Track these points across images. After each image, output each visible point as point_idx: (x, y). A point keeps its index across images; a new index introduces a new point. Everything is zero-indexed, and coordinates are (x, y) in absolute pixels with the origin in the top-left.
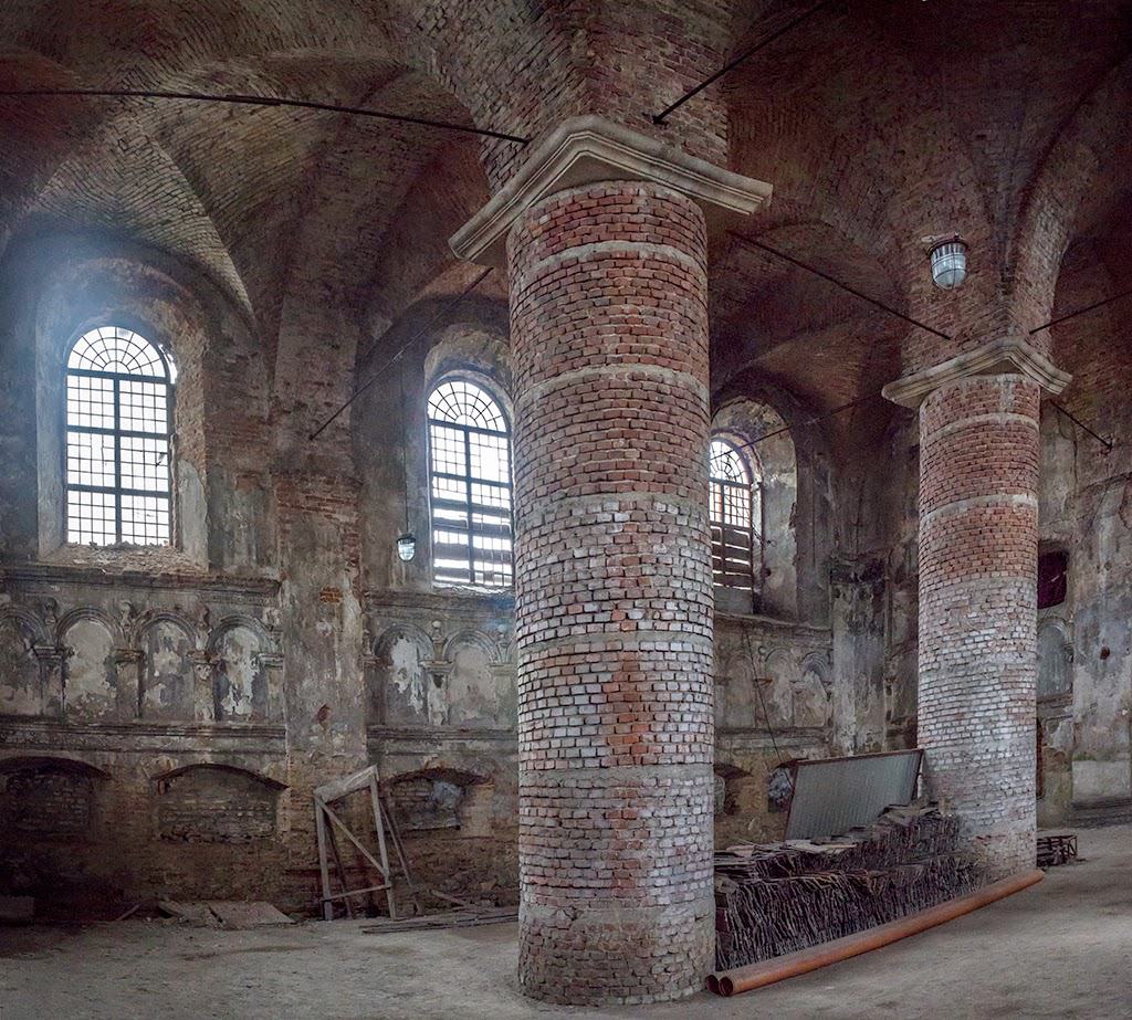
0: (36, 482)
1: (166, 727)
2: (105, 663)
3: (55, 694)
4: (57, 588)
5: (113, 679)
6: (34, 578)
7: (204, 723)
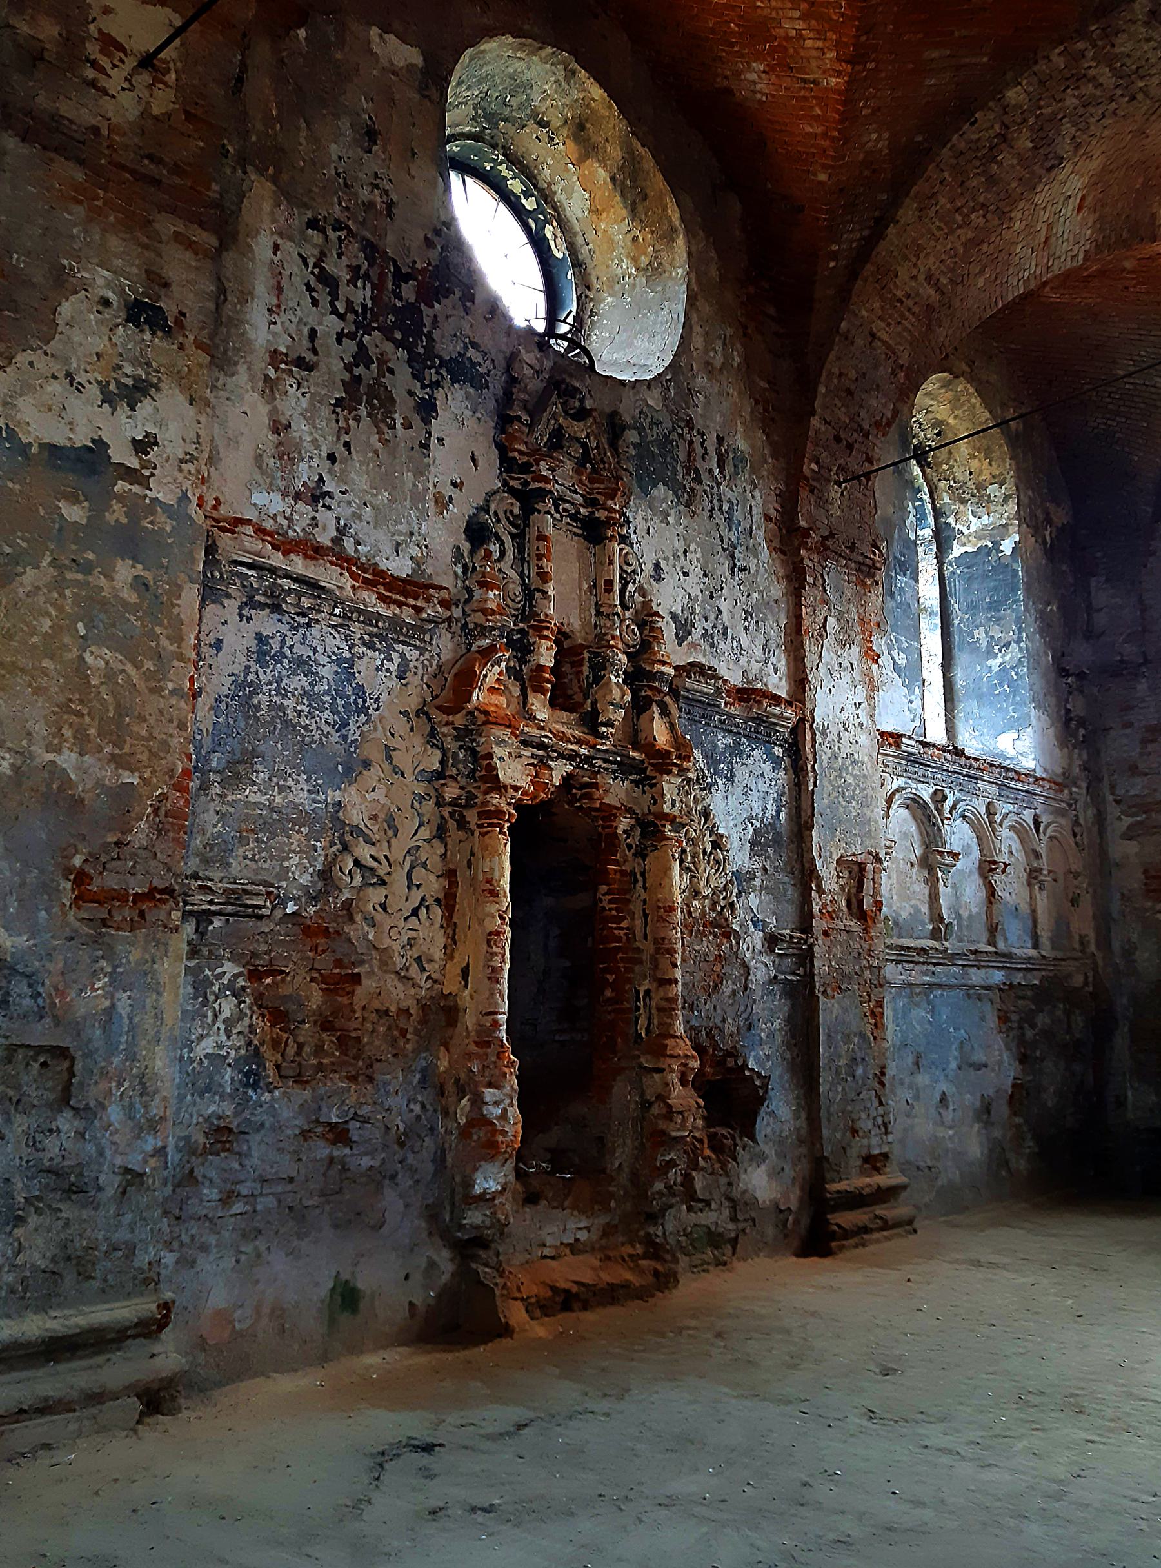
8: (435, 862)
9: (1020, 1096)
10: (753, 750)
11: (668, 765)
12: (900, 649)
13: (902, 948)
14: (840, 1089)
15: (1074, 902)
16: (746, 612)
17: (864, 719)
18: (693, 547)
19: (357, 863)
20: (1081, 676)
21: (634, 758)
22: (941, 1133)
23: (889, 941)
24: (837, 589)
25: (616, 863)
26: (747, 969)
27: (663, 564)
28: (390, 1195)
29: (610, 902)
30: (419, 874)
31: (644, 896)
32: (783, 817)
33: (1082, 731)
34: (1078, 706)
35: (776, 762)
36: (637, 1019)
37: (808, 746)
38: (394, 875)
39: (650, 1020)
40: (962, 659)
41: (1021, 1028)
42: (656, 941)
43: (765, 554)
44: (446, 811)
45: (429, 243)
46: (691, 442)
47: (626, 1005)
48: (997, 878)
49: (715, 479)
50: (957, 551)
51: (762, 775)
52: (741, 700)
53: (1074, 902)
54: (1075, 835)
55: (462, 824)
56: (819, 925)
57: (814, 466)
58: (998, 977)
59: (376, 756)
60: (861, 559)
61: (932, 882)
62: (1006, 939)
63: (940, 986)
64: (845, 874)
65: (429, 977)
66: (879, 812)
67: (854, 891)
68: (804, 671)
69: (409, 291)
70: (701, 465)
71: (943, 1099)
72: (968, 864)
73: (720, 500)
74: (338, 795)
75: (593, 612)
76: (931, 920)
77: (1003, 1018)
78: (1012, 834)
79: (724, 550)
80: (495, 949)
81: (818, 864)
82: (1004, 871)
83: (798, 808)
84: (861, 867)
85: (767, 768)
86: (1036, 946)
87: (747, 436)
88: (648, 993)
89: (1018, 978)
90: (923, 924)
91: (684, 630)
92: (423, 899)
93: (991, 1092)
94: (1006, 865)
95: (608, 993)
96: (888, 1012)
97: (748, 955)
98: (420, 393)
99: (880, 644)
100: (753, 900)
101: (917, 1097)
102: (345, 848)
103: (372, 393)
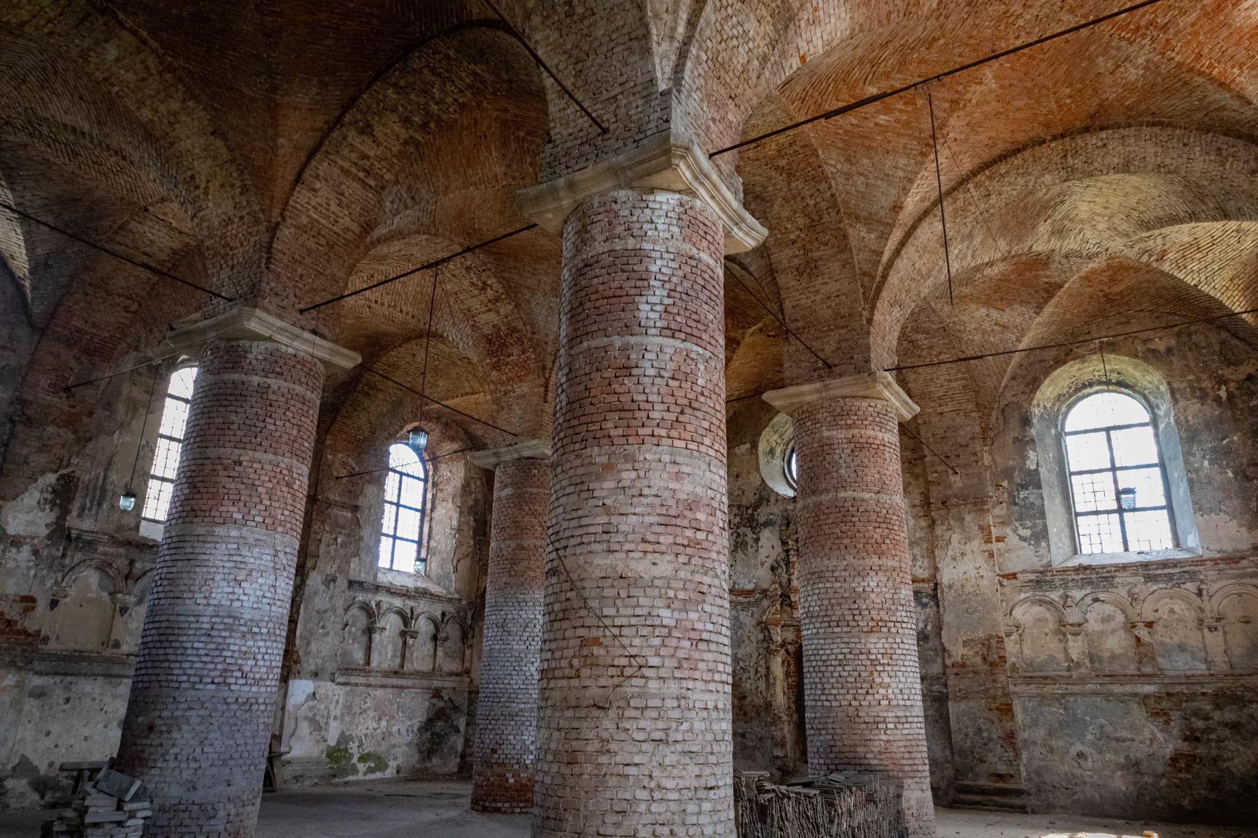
8: (764, 665)
28: (757, 753)
30: (759, 669)
45: (755, 494)
69: (750, 511)
98: (754, 536)
103: (741, 544)
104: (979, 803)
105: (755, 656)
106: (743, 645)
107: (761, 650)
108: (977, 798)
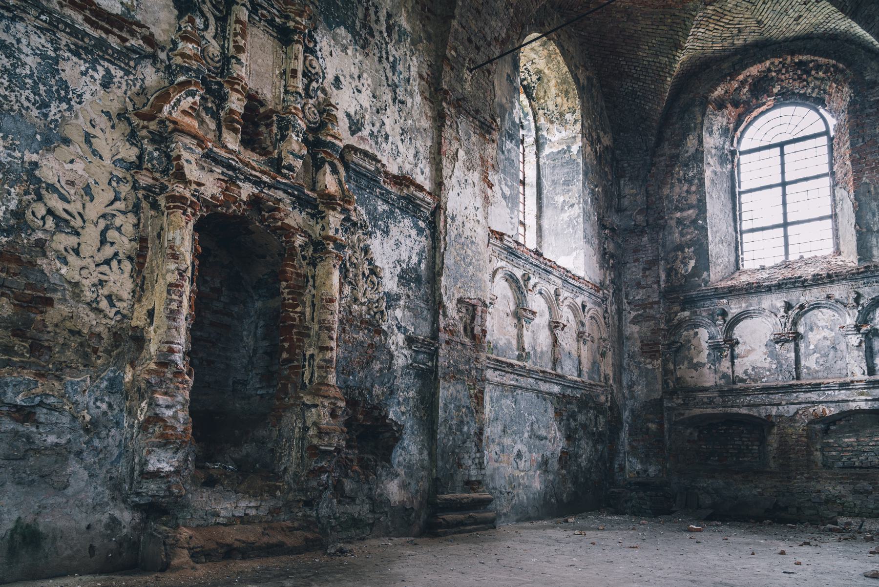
0: (707, 235)
1: (820, 384)
2: (766, 345)
3: (726, 370)
4: (725, 301)
5: (772, 355)
6: (706, 298)
7: (856, 378)
8: (128, 228)
9: (565, 458)
10: (403, 218)
11: (333, 204)
12: (506, 185)
13: (498, 361)
14: (451, 438)
15: (603, 355)
16: (403, 130)
17: (480, 217)
18: (365, 75)
19: (50, 212)
20: (613, 230)
21: (308, 195)
22: (516, 473)
23: (489, 355)
24: (467, 134)
25: (294, 267)
26: (392, 357)
27: (342, 78)
29: (289, 293)
30: (112, 234)
31: (314, 292)
32: (423, 266)
33: (611, 261)
34: (610, 247)
35: (420, 231)
36: (303, 373)
37: (442, 224)
38: (86, 229)
39: (312, 374)
40: (547, 213)
41: (568, 420)
42: (319, 322)
43: (418, 98)
44: (141, 194)
46: (367, 9)
47: (296, 363)
48: (558, 332)
49: (384, 38)
50: (547, 151)
51: (409, 236)
52: (396, 183)
53: (603, 355)
54: (605, 318)
55: (155, 206)
56: (443, 336)
57: (453, 52)
58: (556, 389)
59: (77, 137)
60: (482, 119)
61: (520, 327)
62: (562, 368)
63: (521, 388)
64: (464, 310)
65: (117, 313)
66: (487, 277)
67: (468, 322)
68: (441, 178)
70: (375, 27)
71: (519, 455)
72: (542, 320)
73: (387, 53)
74: (35, 157)
75: (282, 90)
76: (518, 349)
77: (558, 413)
78: (569, 310)
79: (389, 85)
80: (173, 296)
81: (445, 298)
82: (563, 329)
83: (434, 262)
84: (474, 306)
85: (413, 232)
86: (579, 376)
87: (409, 20)
88: (312, 356)
89: (569, 392)
90: (513, 351)
91: (355, 127)
92: (116, 254)
93: (548, 453)
94: (565, 326)
95: (285, 355)
96: (487, 398)
97: (393, 348)
99: (493, 177)
100: (399, 313)
101: (503, 451)
102: (40, 198)
104: (460, 524)
105: (103, 196)
106: (64, 151)
107: (125, 189)
108: (459, 516)
